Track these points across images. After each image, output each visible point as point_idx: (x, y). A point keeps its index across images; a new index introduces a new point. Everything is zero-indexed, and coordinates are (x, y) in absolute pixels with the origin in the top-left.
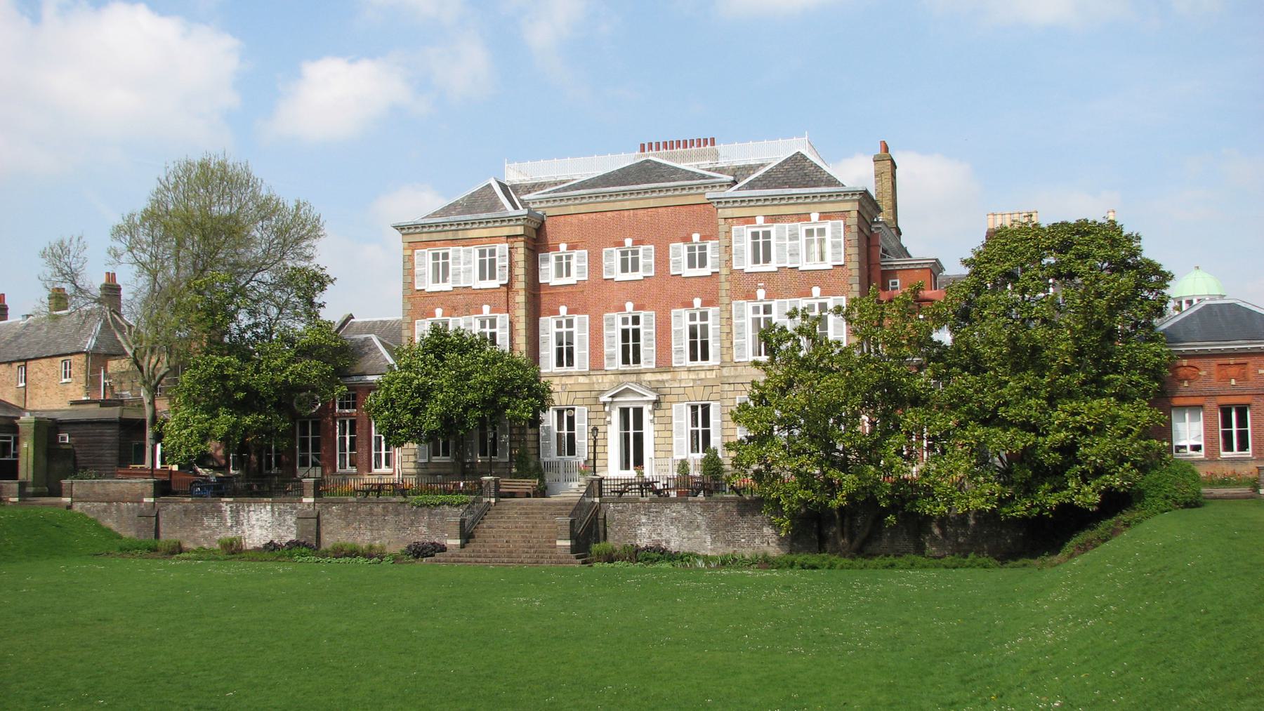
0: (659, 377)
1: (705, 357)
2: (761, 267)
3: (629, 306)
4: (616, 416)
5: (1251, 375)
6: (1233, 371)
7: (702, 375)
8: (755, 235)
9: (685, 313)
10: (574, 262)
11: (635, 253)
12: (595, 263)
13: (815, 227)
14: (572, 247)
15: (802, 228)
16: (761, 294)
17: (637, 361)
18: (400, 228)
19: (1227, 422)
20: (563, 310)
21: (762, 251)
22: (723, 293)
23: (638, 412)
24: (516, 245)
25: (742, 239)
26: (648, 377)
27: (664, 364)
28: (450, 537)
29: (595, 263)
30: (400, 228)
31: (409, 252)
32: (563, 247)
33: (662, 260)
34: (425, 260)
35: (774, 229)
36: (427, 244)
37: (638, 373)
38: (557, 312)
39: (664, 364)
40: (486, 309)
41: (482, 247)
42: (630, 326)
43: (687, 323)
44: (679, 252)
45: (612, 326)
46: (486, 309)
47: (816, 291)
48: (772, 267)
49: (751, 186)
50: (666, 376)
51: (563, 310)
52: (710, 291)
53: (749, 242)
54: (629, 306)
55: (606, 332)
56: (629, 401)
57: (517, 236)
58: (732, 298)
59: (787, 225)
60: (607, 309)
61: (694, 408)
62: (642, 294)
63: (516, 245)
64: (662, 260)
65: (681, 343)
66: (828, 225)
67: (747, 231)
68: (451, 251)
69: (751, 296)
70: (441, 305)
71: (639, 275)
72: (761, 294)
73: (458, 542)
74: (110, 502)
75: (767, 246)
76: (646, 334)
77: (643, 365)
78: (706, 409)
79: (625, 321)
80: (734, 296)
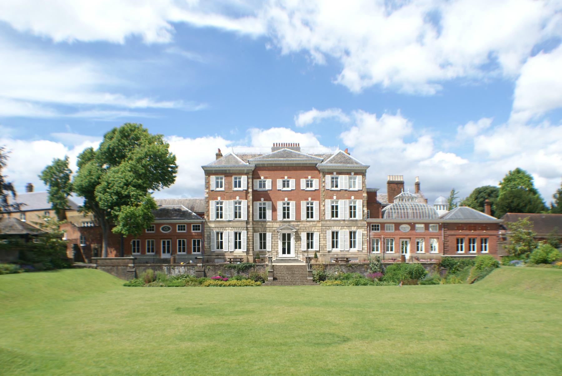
0: (296, 223)
1: (312, 217)
2: (334, 189)
3: (286, 199)
7: (311, 223)
8: (333, 178)
10: (266, 183)
14: (265, 178)
15: (347, 176)
17: (288, 217)
18: (203, 167)
20: (262, 199)
23: (289, 235)
24: (249, 176)
26: (292, 223)
27: (298, 219)
28: (269, 277)
30: (203, 167)
33: (298, 184)
34: (213, 178)
37: (289, 222)
38: (260, 200)
39: (298, 219)
40: (238, 198)
41: (236, 176)
46: (238, 198)
48: (338, 189)
49: (331, 161)
50: (299, 223)
51: (262, 199)
52: (315, 195)
54: (286, 199)
59: (344, 176)
60: (279, 200)
62: (292, 195)
63: (249, 176)
64: (298, 184)
69: (331, 198)
70: (220, 196)
73: (272, 278)
77: (290, 219)
78: (312, 234)
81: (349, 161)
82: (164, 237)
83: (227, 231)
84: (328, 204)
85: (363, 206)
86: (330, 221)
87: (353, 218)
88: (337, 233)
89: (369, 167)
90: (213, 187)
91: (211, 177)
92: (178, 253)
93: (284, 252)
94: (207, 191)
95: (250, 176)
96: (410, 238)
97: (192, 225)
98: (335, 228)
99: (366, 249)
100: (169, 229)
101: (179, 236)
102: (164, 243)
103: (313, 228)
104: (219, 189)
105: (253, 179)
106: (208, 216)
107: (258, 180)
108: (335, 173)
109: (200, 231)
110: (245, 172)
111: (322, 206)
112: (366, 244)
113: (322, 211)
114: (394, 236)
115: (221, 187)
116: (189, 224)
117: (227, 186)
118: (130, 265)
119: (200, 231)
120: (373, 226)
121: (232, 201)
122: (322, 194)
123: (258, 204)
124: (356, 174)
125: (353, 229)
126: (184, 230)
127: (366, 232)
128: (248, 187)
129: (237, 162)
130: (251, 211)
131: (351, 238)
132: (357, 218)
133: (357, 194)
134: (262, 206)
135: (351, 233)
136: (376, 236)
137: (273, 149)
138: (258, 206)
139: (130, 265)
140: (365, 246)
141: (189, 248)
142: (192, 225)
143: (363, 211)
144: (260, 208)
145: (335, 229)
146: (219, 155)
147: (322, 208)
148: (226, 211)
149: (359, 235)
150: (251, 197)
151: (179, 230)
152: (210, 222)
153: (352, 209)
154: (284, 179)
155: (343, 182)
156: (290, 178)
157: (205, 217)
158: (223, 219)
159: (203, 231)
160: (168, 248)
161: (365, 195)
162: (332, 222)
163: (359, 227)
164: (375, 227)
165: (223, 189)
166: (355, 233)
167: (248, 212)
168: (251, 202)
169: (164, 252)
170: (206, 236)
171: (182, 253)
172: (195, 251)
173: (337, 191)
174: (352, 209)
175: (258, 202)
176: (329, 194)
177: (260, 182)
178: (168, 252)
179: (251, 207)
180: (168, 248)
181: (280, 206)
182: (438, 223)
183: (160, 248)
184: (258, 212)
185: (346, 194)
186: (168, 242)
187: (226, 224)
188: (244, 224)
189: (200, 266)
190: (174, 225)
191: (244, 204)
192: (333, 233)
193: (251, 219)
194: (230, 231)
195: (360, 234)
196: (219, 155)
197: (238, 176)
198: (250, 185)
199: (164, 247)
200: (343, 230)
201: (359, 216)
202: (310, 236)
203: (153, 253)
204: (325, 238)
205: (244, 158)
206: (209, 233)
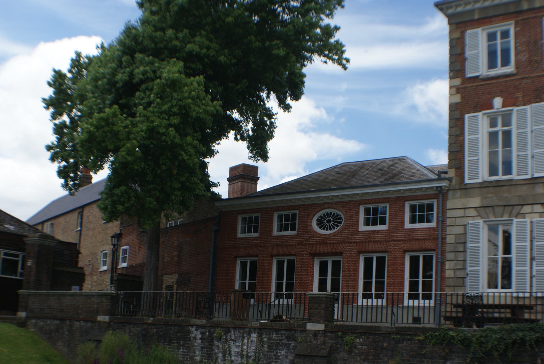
31: (457, 35)
34: (478, 41)
74: (62, 320)
83: (528, 220)
90: (479, 66)
91: (469, 32)
94: (457, 82)
104: (500, 70)
115: (506, 62)
117: (524, 57)
118: (100, 318)
119: (433, 225)
126: (383, 222)
139: (100, 318)
148: (523, 145)
151: (367, 223)
152: (466, 190)
158: (515, 176)
159: (442, 222)
165: (510, 69)
170: (450, 239)
186: (336, 265)
187: (524, 190)
189: (316, 333)
194: (536, 218)
206: (460, 230)
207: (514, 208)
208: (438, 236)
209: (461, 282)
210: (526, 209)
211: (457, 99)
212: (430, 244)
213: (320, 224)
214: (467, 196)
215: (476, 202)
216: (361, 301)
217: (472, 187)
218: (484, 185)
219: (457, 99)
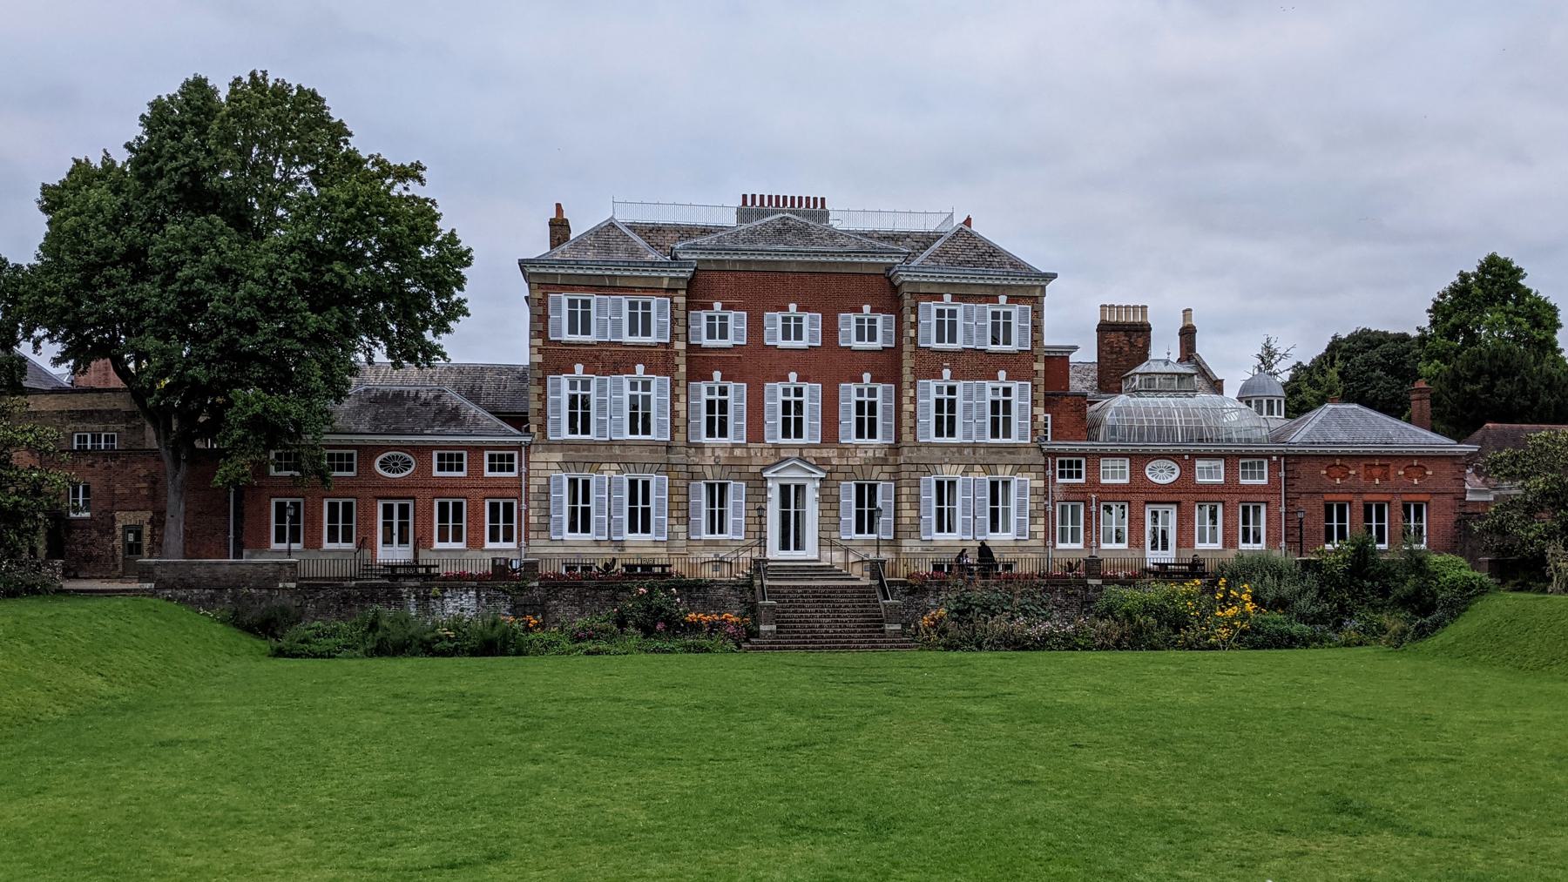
2: (946, 346)
3: (793, 376)
4: (774, 495)
5: (1392, 475)
6: (1376, 471)
9: (854, 387)
11: (799, 319)
12: (756, 327)
13: (1002, 311)
16: (947, 373)
19: (1368, 518)
20: (717, 375)
21: (947, 328)
22: (906, 371)
23: (800, 489)
24: (676, 300)
25: (928, 313)
29: (756, 327)
30: (523, 264)
31: (539, 295)
32: (718, 306)
33: (830, 330)
34: (561, 304)
35: (960, 308)
36: (564, 287)
38: (710, 378)
42: (792, 398)
43: (855, 398)
44: (848, 324)
45: (774, 398)
47: (1002, 374)
48: (959, 345)
51: (717, 375)
53: (934, 318)
55: (767, 403)
56: (792, 476)
57: (676, 290)
58: (917, 377)
61: (860, 488)
64: (830, 330)
65: (848, 421)
66: (1015, 310)
67: (934, 306)
68: (594, 299)
71: (803, 344)
72: (947, 373)
75: (953, 325)
76: (810, 407)
78: (873, 488)
79: (786, 392)
80: (918, 374)
81: (989, 255)
82: (386, 490)
83: (606, 475)
84: (930, 391)
85: (1034, 403)
86: (929, 445)
87: (1001, 440)
88: (952, 484)
89: (1054, 276)
92: (437, 545)
93: (785, 546)
94: (539, 342)
95: (681, 300)
96: (1178, 503)
97: (486, 454)
98: (946, 468)
99: (1041, 536)
100: (407, 465)
101: (440, 487)
102: (388, 511)
103: (877, 469)
105: (689, 306)
106: (542, 427)
107: (704, 314)
108: (947, 298)
109: (514, 474)
110: (665, 284)
111: (905, 400)
112: (1042, 521)
113: (905, 416)
114: (1128, 497)
116: (477, 450)
119: (514, 474)
120: (1062, 464)
121: (626, 380)
122: (908, 363)
123: (701, 392)
124: (1012, 300)
125: (1003, 473)
126: (460, 468)
127: (1041, 484)
128: (674, 336)
129: (634, 251)
130: (683, 414)
131: (994, 500)
132: (1014, 439)
133: (1017, 365)
134: (717, 397)
135: (994, 485)
136: (1071, 497)
137: (744, 213)
138: (705, 396)
140: (1039, 528)
141: (477, 528)
142: (486, 454)
143: (1034, 418)
144: (710, 404)
145: (948, 472)
146: (559, 228)
147: (908, 407)
149: (1021, 493)
150: (683, 369)
152: (550, 446)
153: (1000, 412)
154: (786, 314)
155: (972, 327)
156: (807, 309)
157: (533, 428)
160: (403, 526)
161: (1039, 366)
162: (938, 452)
163: (1020, 468)
164: (1070, 466)
166: (1006, 484)
167: (674, 414)
168: (682, 383)
169: (388, 541)
170: (533, 489)
171: (451, 545)
172: (494, 538)
173: (955, 352)
174: (1000, 412)
175: (704, 386)
176: (930, 364)
177: (711, 318)
178: (403, 540)
179: (683, 398)
180: (403, 526)
181: (775, 395)
182: (1269, 457)
183: (373, 529)
184: (704, 415)
185: (977, 365)
186: (404, 511)
188: (661, 457)
190: (422, 451)
191: (659, 390)
192: (940, 484)
193: (680, 437)
195: (1023, 486)
196: (559, 228)
197: (640, 300)
198: (680, 330)
199: (388, 526)
200: (971, 477)
201: (1018, 434)
202: (866, 494)
203: (351, 546)
204: (916, 502)
205: (659, 240)
206: (544, 482)
207: (594, 465)
208: (517, 486)
209: (546, 528)
210: (604, 467)
211: (539, 358)
212: (514, 493)
213: (383, 465)
214: (550, 451)
215: (558, 457)
216: (437, 545)
217: (554, 443)
218: (564, 444)
219: (539, 358)
